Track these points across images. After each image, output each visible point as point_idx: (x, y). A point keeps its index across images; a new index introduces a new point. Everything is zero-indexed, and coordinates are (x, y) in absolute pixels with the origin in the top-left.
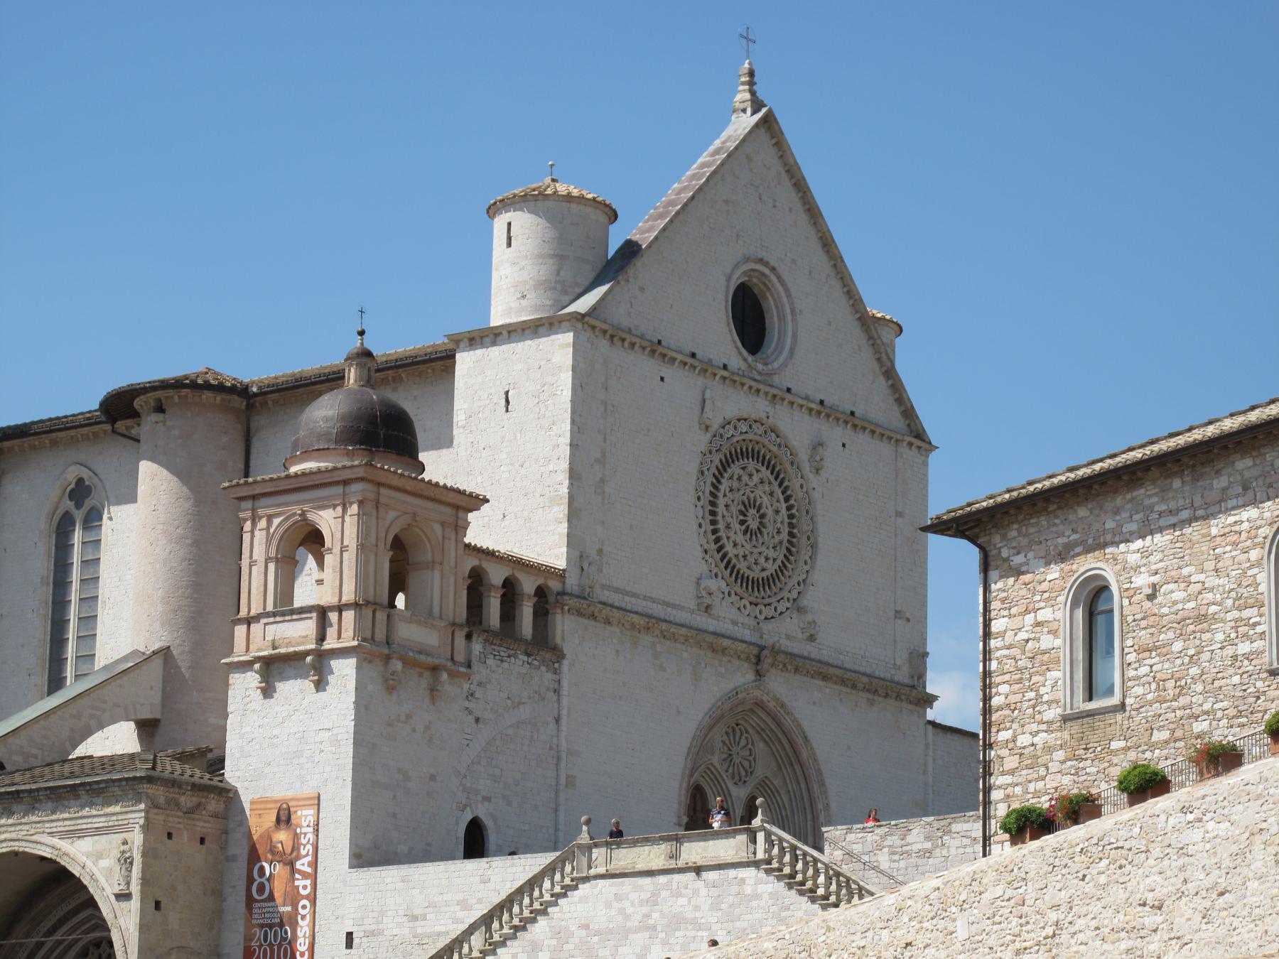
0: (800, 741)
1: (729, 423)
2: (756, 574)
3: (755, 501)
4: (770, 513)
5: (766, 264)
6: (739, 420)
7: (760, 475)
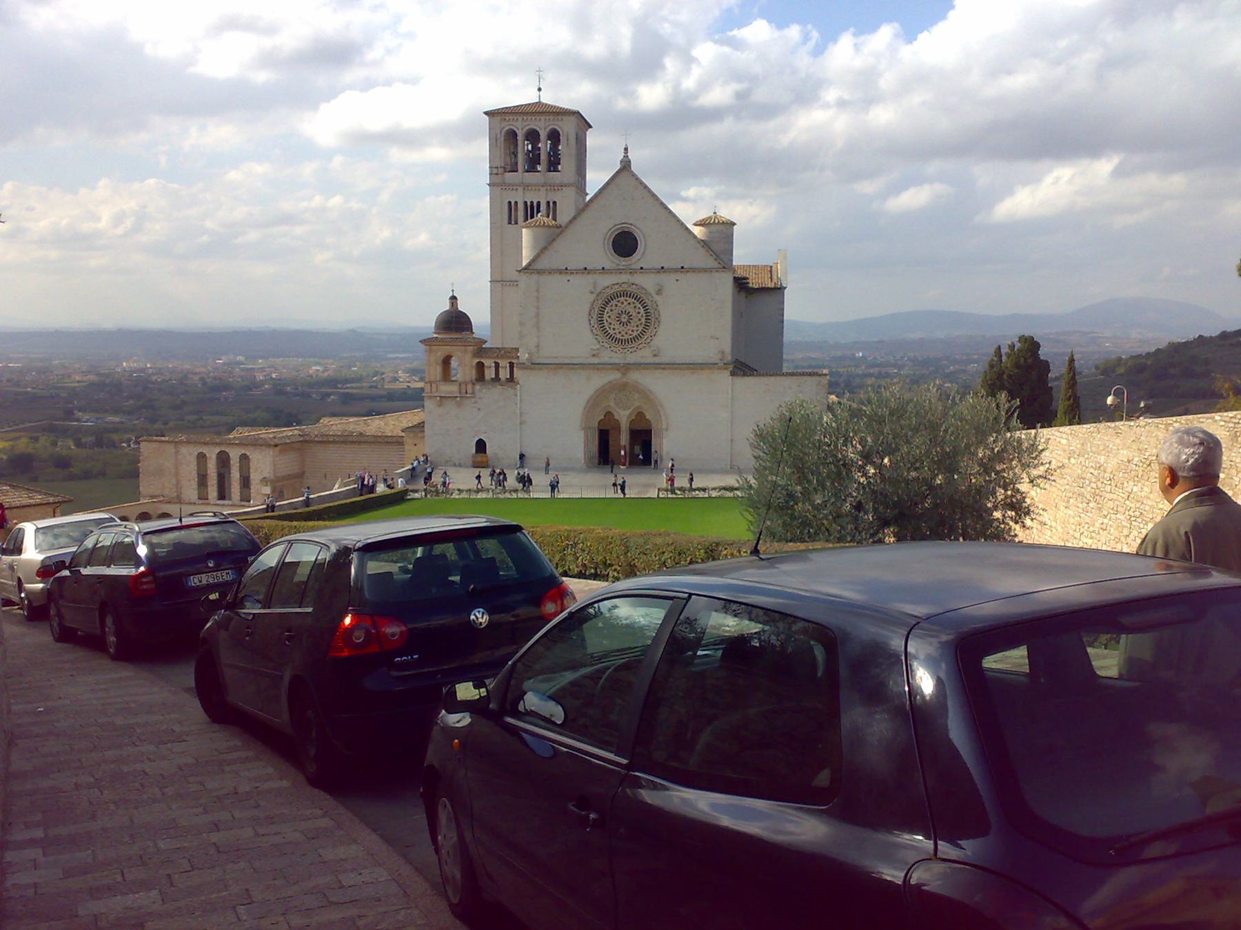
0: (649, 393)
2: (626, 337)
4: (634, 314)
5: (626, 223)
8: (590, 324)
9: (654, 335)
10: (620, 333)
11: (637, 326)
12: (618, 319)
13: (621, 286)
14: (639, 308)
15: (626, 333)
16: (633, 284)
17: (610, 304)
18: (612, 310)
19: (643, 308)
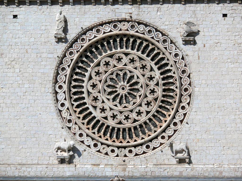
1: (91, 29)
2: (128, 124)
3: (125, 74)
4: (142, 80)
6: (102, 25)
7: (130, 57)
8: (57, 100)
9: (181, 121)
10: (114, 117)
11: (148, 104)
12: (109, 90)
13: (115, 26)
14: (152, 70)
15: (127, 118)
16: (139, 23)
17: (96, 61)
18: (98, 73)
19: (159, 68)
